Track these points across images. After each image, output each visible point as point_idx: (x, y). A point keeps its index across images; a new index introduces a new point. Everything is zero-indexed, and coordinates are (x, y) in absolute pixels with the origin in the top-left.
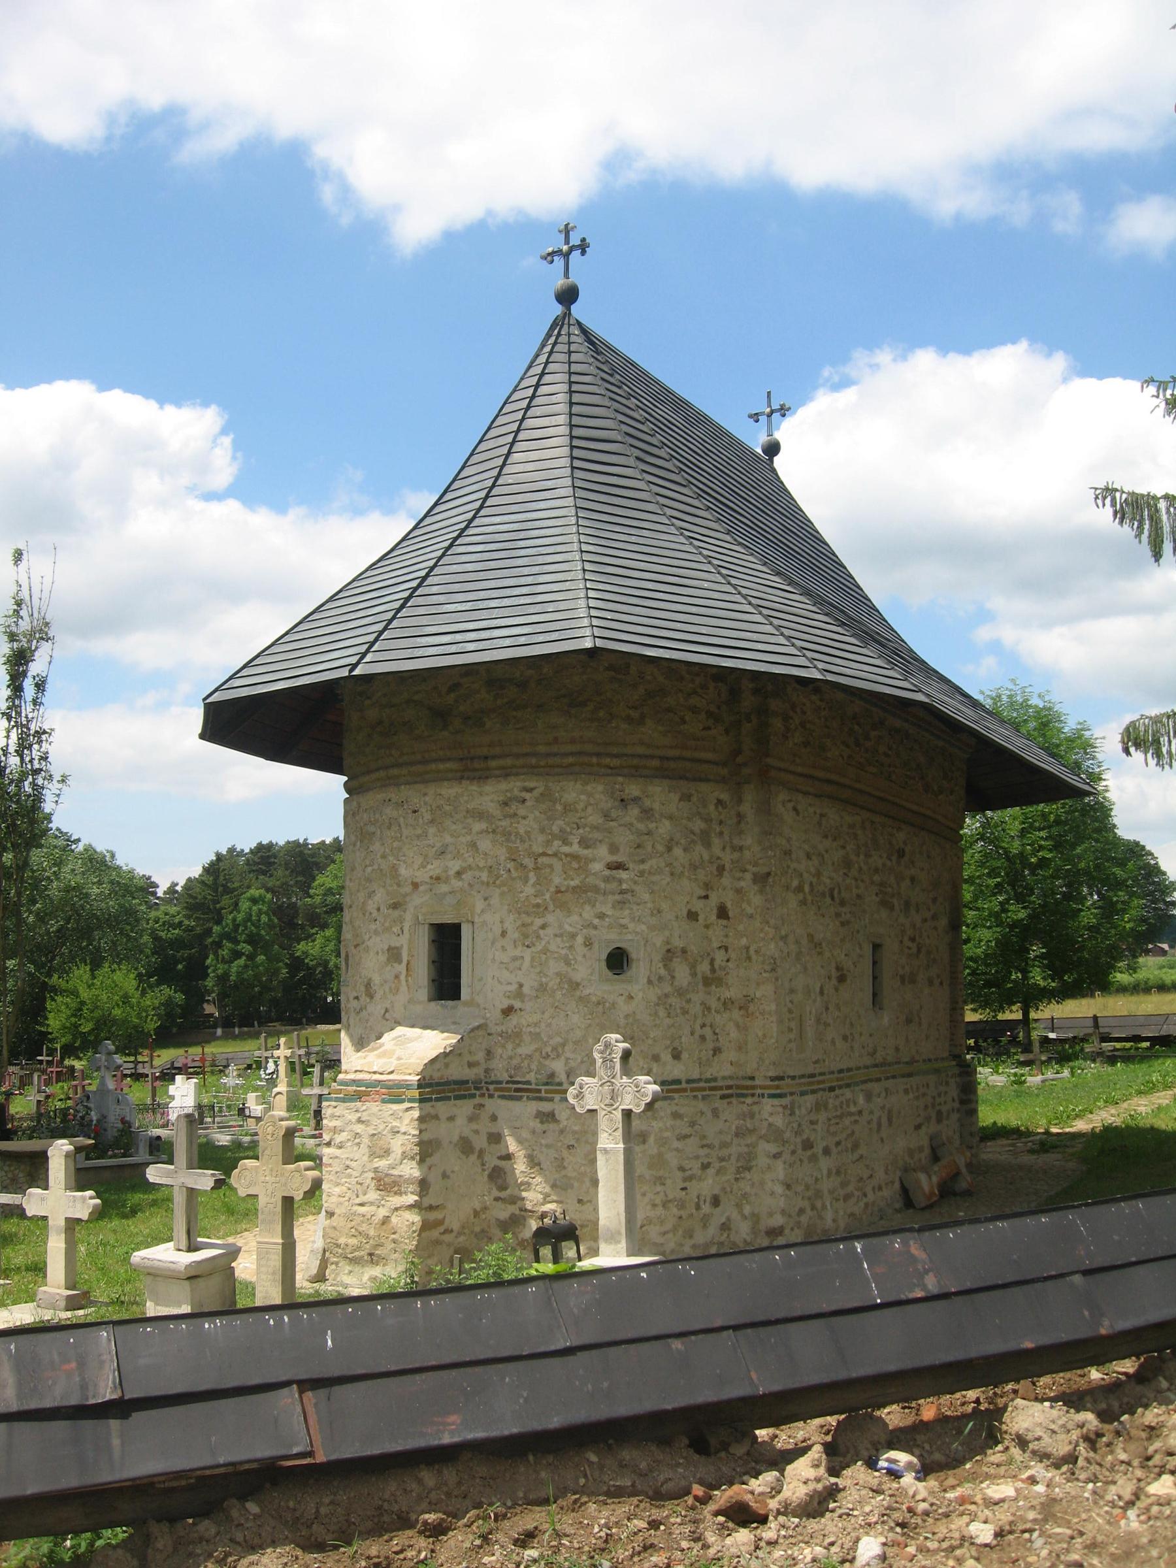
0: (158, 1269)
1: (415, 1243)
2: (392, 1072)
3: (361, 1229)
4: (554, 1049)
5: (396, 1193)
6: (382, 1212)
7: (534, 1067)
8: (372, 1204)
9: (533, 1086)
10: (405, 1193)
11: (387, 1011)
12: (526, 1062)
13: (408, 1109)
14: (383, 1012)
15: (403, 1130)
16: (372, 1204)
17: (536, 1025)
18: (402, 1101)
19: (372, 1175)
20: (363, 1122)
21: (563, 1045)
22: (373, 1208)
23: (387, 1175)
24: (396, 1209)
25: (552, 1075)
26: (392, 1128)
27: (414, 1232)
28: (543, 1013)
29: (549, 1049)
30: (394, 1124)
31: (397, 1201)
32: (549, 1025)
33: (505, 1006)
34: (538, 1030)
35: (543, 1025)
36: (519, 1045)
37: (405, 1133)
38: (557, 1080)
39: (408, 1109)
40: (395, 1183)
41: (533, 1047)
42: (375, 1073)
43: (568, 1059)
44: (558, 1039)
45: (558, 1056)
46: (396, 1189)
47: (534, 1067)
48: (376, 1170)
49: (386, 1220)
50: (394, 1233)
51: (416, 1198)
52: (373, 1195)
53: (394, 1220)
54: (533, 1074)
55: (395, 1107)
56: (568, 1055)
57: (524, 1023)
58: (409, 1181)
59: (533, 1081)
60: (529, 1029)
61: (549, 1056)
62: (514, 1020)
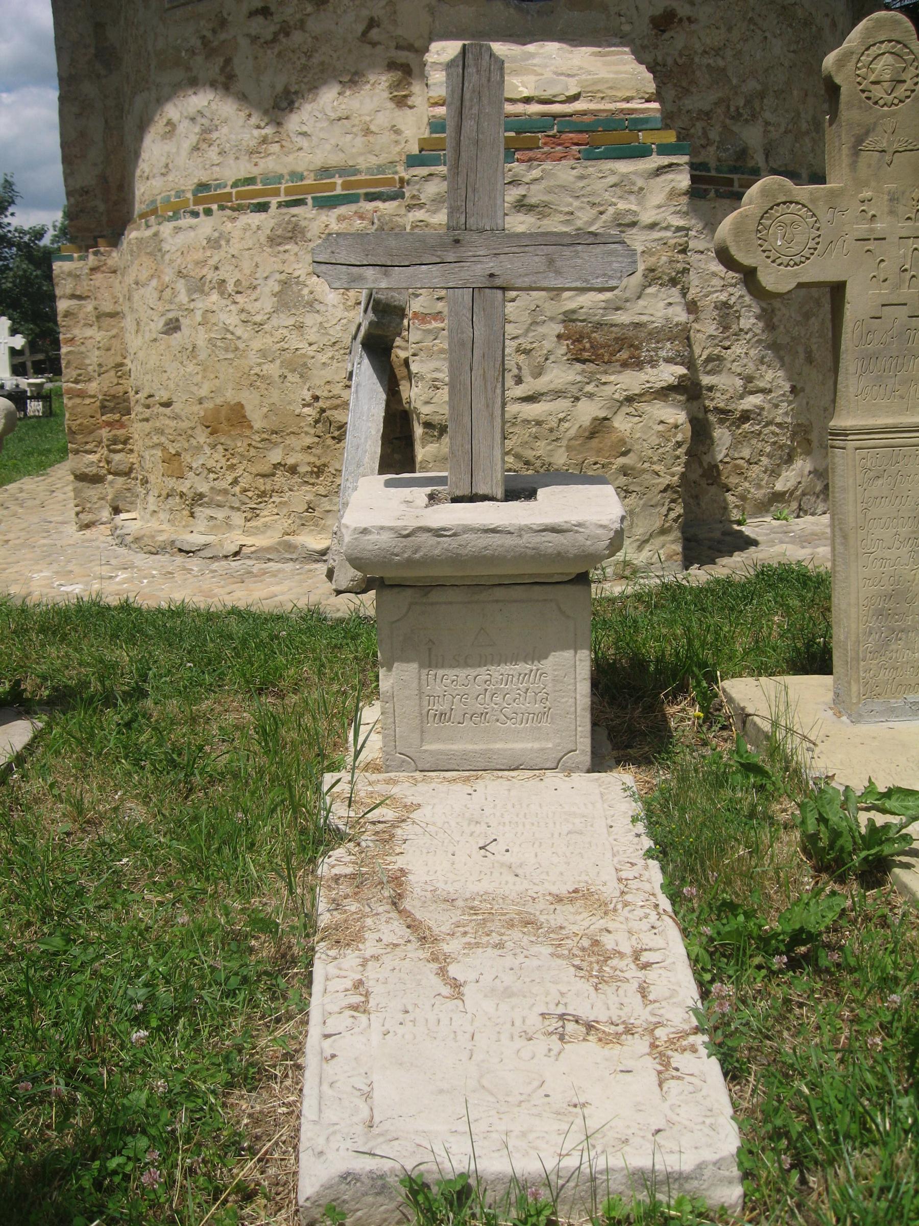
0: (480, 559)
1: (679, 469)
2: (575, 98)
3: (529, 454)
4: (748, 102)
5: (625, 365)
6: (587, 411)
7: (714, 135)
8: (558, 394)
9: (713, 173)
10: (653, 363)
11: (372, 23)
12: (699, 125)
13: (659, 171)
14: (360, 28)
15: (647, 217)
16: (558, 394)
17: (718, 52)
18: (643, 152)
19: (559, 328)
20: (531, 208)
21: (762, 95)
22: (563, 404)
23: (599, 325)
24: (630, 400)
25: (743, 153)
26: (618, 215)
27: (679, 444)
28: (730, 29)
29: (741, 103)
30: (622, 206)
31: (632, 381)
32: (738, 55)
33: (658, 11)
34: (721, 63)
35: (729, 53)
36: (687, 92)
37: (653, 226)
38: (751, 164)
39: (659, 171)
40: (622, 342)
41: (713, 96)
42: (527, 100)
43: (767, 123)
44: (752, 85)
45: (754, 116)
46: (624, 355)
47: (714, 135)
48: (569, 318)
49: (599, 427)
50: (624, 454)
51: (681, 370)
52: (561, 375)
53: (622, 424)
54: (712, 149)
55: (624, 167)
56: (767, 115)
57: (698, 47)
58: (661, 335)
59: (713, 164)
60: (706, 61)
61: (740, 115)
62: (678, 39)
